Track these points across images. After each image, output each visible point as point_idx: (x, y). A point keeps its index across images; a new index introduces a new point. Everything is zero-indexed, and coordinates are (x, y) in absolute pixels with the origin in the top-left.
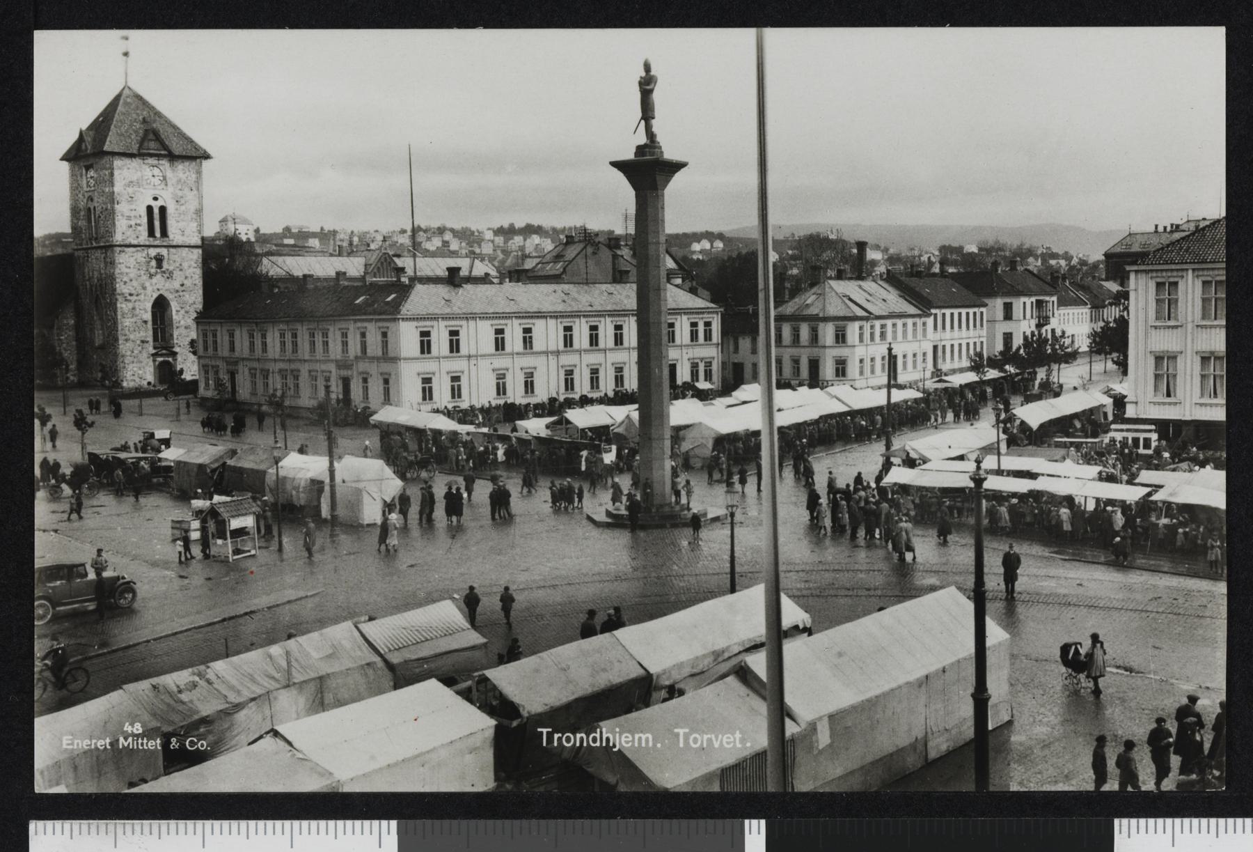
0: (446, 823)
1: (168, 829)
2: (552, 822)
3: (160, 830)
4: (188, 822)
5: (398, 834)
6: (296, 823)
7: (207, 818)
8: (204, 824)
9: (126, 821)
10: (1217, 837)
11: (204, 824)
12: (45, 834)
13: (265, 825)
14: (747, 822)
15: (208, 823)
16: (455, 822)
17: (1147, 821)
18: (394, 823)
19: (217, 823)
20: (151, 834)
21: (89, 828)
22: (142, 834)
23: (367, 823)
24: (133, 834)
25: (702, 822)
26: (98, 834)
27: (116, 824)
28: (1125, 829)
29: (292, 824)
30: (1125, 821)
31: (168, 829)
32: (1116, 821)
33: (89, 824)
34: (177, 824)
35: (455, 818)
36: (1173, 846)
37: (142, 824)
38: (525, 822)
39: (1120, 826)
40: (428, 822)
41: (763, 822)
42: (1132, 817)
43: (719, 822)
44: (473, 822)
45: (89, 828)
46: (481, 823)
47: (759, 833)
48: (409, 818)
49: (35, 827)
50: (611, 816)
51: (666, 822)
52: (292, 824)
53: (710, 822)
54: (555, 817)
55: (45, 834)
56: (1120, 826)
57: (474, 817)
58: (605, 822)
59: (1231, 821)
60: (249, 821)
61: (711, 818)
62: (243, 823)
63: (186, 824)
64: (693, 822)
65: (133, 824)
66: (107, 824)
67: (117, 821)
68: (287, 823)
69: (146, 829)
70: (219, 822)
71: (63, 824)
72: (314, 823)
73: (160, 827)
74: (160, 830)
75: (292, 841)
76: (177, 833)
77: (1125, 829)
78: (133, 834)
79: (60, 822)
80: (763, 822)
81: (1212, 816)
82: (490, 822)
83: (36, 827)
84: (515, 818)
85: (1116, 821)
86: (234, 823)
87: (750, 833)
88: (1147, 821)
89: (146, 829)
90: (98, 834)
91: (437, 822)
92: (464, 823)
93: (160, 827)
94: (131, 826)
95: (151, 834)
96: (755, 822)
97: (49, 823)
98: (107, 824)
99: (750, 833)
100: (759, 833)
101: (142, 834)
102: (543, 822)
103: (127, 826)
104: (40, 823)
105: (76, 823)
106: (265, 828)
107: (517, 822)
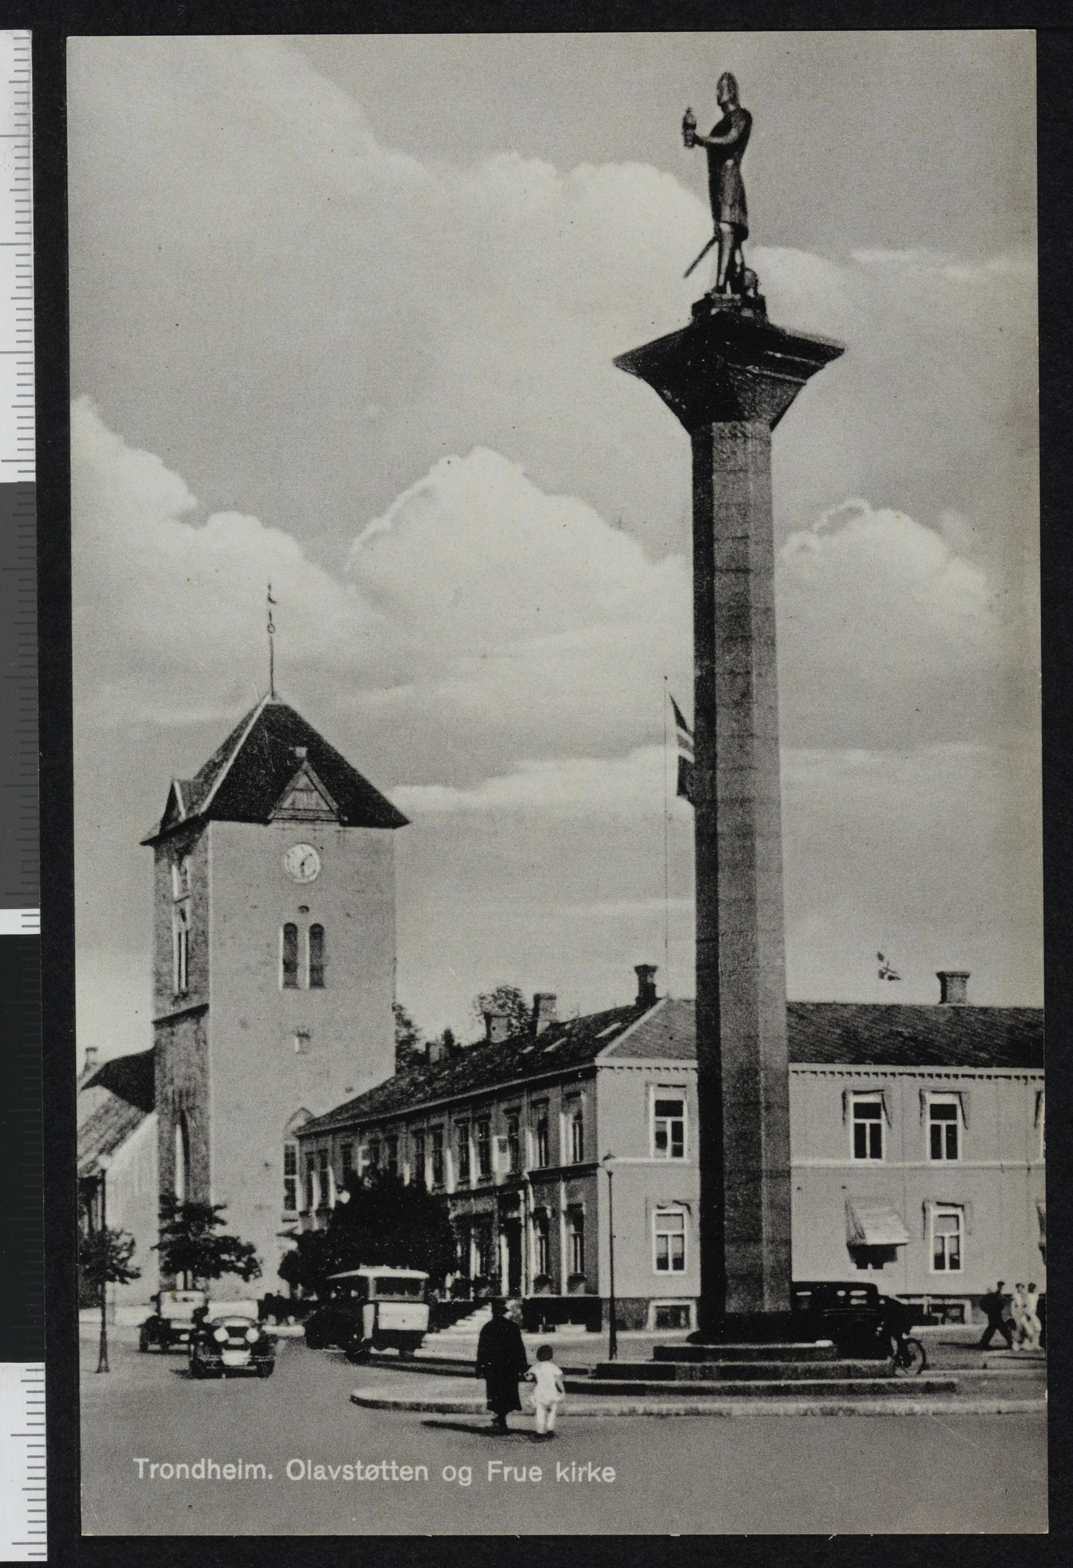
0: (33, 542)
1: (22, 201)
2: (35, 672)
3: (21, 190)
4: (32, 225)
5: (20, 483)
6: (31, 358)
7: (36, 249)
8: (30, 244)
9: (31, 149)
10: (24, 1489)
11: (30, 244)
12: (16, 49)
13: (29, 320)
14: (37, 911)
15: (30, 250)
16: (33, 552)
17: (43, 1402)
18: (32, 477)
19: (30, 260)
20: (17, 179)
21: (24, 104)
22: (16, 168)
23: (32, 444)
24: (17, 158)
25: (37, 856)
26: (16, 114)
27: (28, 136)
28: (33, 1376)
29: (30, 352)
30: (42, 1376)
31: (22, 201)
32: (42, 1365)
33: (28, 103)
34: (29, 211)
35: (39, 552)
36: (12, 1435)
37: (28, 168)
38: (34, 639)
39: (37, 1370)
40: (34, 520)
41: (37, 931)
42: (47, 1384)
43: (37, 877)
44: (34, 574)
45: (24, 104)
46: (34, 585)
47: (24, 926)
48: (39, 496)
49: (26, 34)
50: (43, 745)
51: (36, 813)
52: (30, 352)
53: (37, 867)
54: (41, 675)
55: (16, 49)
56: (37, 1370)
57: (40, 576)
58: (36, 737)
59: (43, 1505)
60: (32, 301)
61: (42, 868)
62: (30, 293)
63: (29, 222)
64: (36, 845)
65: (28, 157)
66: (28, 125)
67: (32, 138)
68: (31, 347)
69: (22, 174)
70: (32, 263)
71: (28, 71)
72: (31, 379)
73: (24, 190)
74: (21, 190)
75: (9, 353)
76: (17, 212)
77: (33, 1376)
78: (17, 158)
79: (31, 68)
80: (37, 931)
81: (49, 1483)
82: (34, 596)
83: (23, 38)
84: (41, 626)
85: (42, 1365)
86: (30, 282)
87: (23, 916)
88: (43, 1402)
89: (22, 174)
90: (16, 114)
91: (33, 531)
92: (33, 564)
93: (24, 190)
94: (26, 155)
95: (17, 179)
96: (37, 921)
97: (28, 54)
98: (28, 125)
99: (23, 916)
100: (24, 926)
101: (16, 168)
102: (35, 661)
103: (25, 150)
104: (28, 44)
105: (29, 87)
106: (25, 320)
107: (34, 628)
